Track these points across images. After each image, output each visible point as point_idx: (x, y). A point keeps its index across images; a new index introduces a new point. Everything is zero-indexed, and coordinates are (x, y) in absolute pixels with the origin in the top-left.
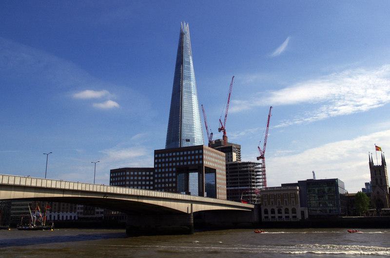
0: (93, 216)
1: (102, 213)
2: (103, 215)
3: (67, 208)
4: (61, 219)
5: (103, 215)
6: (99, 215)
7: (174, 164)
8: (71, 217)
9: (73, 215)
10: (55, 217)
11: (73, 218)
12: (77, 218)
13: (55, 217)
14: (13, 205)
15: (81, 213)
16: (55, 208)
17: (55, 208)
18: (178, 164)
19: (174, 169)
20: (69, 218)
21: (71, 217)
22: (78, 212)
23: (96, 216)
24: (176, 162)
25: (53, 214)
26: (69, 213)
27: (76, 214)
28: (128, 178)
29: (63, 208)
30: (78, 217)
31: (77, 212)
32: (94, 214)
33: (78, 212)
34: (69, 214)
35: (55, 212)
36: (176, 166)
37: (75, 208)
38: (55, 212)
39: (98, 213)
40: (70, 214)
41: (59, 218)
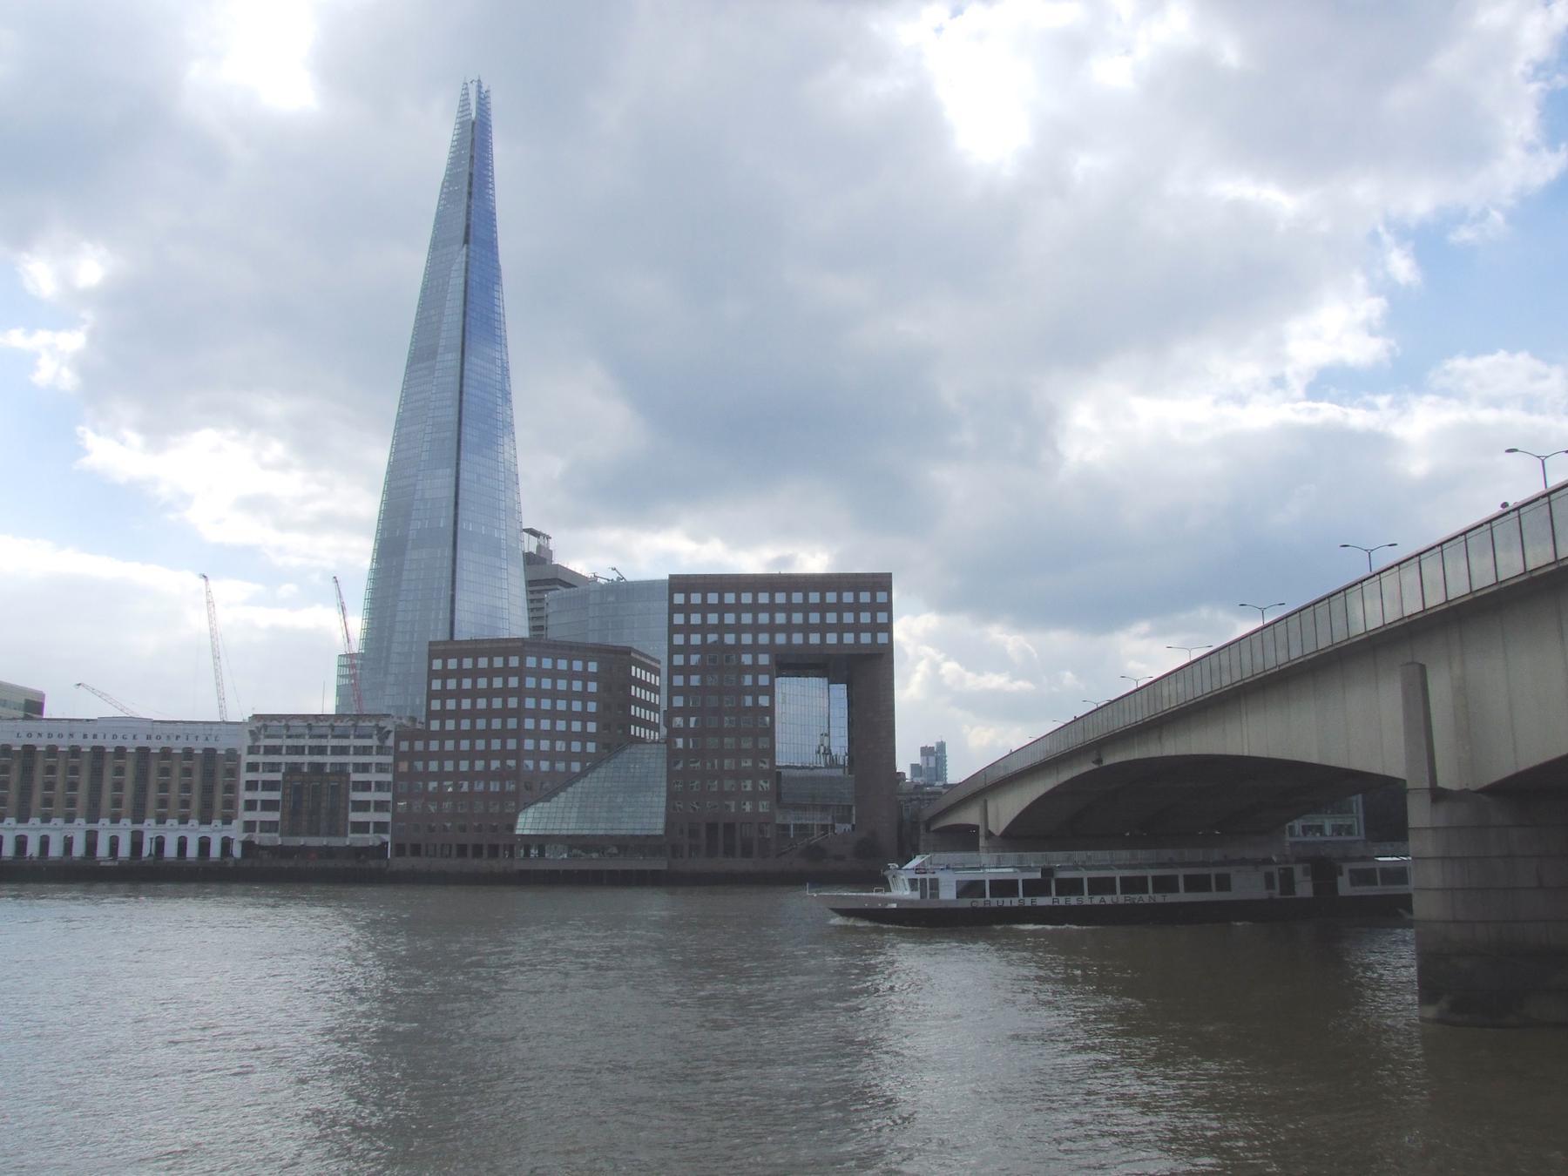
0: (335, 842)
1: (380, 827)
2: (387, 838)
3: (185, 804)
4: (147, 849)
5: (387, 838)
6: (371, 839)
7: (764, 639)
8: (204, 844)
9: (216, 833)
10: (114, 843)
11: (215, 851)
12: (237, 851)
13: (114, 843)
15: (269, 827)
16: (117, 803)
17: (117, 803)
18: (781, 639)
19: (764, 659)
20: (192, 851)
21: (204, 844)
22: (249, 826)
23: (353, 839)
24: (772, 629)
25: (105, 830)
26: (194, 822)
27: (236, 832)
28: (531, 683)
29: (163, 803)
30: (248, 846)
31: (237, 825)
32: (334, 831)
33: (249, 826)
34: (194, 833)
35: (115, 819)
36: (770, 648)
37: (230, 804)
38: (115, 819)
39: (361, 827)
40: (205, 830)
41: (137, 845)
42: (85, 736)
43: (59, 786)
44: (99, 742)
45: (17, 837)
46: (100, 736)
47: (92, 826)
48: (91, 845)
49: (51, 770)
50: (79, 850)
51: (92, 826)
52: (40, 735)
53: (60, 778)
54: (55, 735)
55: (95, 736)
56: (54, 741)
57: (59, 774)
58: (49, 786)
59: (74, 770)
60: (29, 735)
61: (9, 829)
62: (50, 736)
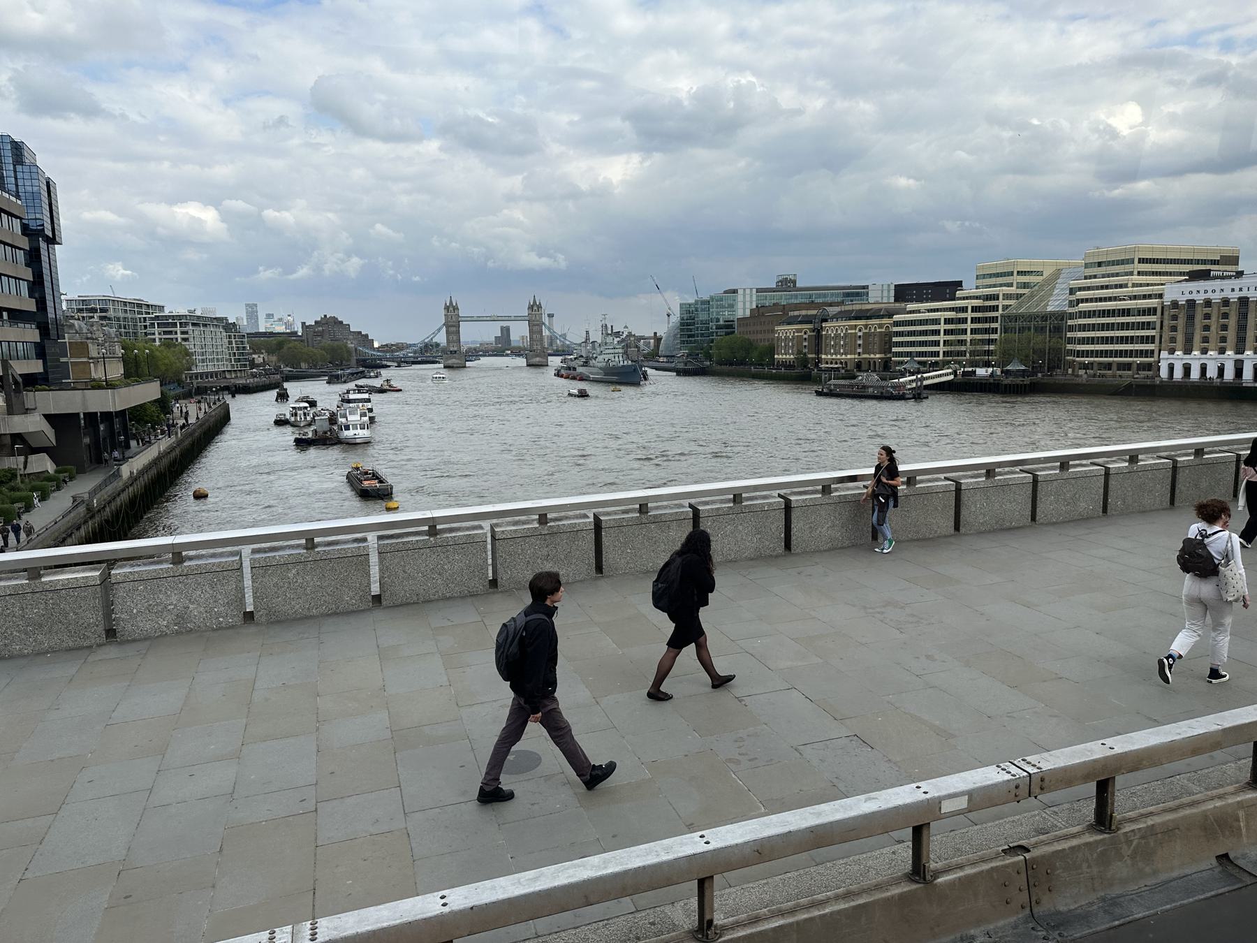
14: (1071, 328)
42: (1233, 290)
43: (1213, 328)
44: (1244, 293)
45: (1184, 364)
46: (1245, 289)
47: (1239, 357)
48: (1239, 372)
49: (1207, 316)
50: (1229, 375)
51: (1239, 357)
52: (1198, 292)
53: (1214, 323)
54: (1210, 291)
55: (1241, 290)
56: (1210, 295)
57: (1214, 318)
58: (1207, 328)
59: (1225, 316)
60: (1191, 292)
61: (1179, 359)
62: (1206, 292)
